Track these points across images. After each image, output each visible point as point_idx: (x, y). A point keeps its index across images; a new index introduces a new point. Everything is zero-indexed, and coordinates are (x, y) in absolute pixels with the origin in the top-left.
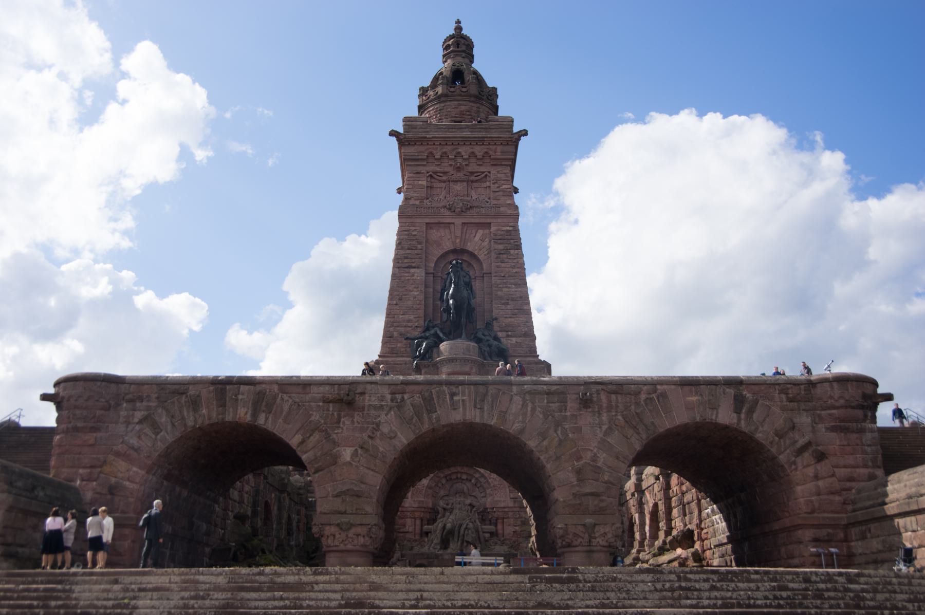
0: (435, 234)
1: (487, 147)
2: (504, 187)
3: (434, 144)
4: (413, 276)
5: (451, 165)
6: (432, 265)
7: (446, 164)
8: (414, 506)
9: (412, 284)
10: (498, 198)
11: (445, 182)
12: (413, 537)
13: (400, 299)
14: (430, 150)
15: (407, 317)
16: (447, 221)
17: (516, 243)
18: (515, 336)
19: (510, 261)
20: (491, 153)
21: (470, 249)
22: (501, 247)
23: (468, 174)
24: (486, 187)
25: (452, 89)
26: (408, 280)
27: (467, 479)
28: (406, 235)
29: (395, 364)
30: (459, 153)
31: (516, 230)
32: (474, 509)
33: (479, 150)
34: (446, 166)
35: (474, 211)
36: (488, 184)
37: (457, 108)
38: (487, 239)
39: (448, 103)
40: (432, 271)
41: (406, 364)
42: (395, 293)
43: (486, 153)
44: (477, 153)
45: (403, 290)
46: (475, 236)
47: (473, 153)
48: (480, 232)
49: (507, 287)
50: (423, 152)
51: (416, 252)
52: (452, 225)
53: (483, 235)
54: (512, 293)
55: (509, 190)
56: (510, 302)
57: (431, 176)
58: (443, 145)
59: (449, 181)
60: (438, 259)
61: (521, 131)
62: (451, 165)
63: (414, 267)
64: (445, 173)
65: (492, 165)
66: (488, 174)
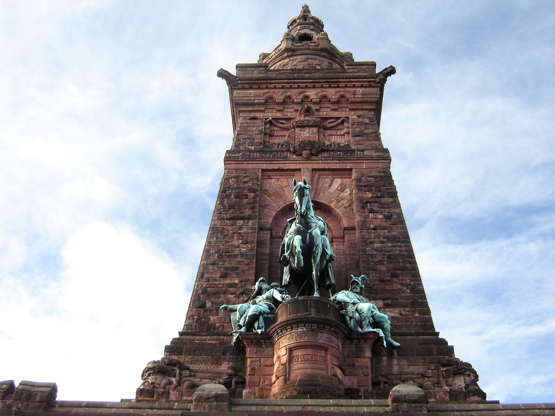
0: (273, 183)
1: (343, 90)
3: (275, 88)
4: (240, 228)
5: (296, 110)
6: (271, 220)
7: (292, 110)
9: (238, 239)
10: (361, 142)
14: (271, 94)
15: (228, 281)
16: (292, 166)
17: (390, 190)
20: (348, 96)
21: (323, 201)
22: (369, 195)
23: (319, 119)
24: (344, 135)
25: (299, 44)
26: (234, 233)
30: (307, 97)
31: (390, 176)
33: (332, 93)
34: (290, 112)
36: (345, 130)
37: (304, 61)
38: (348, 191)
39: (294, 58)
40: (269, 226)
43: (343, 96)
44: (330, 96)
46: (330, 186)
47: (325, 97)
48: (338, 182)
50: (259, 96)
52: (298, 172)
53: (341, 184)
57: (270, 122)
58: (286, 88)
59: (294, 128)
60: (277, 214)
61: (386, 69)
62: (296, 110)
63: (243, 218)
64: (289, 119)
65: (351, 110)
66: (346, 119)
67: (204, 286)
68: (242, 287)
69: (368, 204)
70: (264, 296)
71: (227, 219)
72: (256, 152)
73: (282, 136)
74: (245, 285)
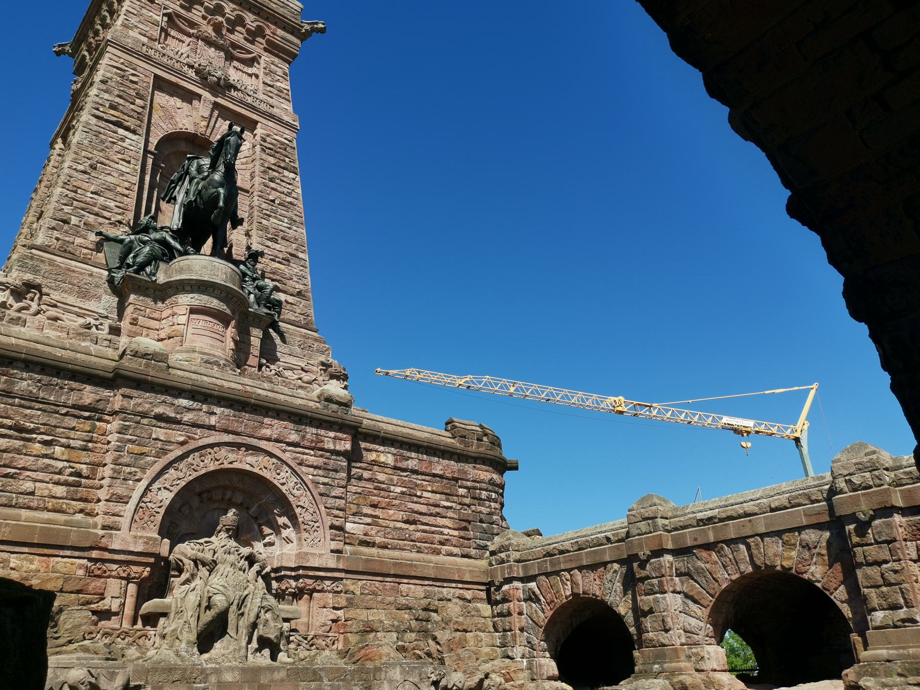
2: (278, 84)
4: (123, 140)
8: (132, 549)
11: (189, 35)
12: (118, 626)
13: (93, 167)
18: (285, 292)
19: (284, 184)
20: (268, 32)
27: (241, 504)
28: (116, 74)
29: (69, 270)
32: (256, 567)
35: (234, 93)
41: (91, 275)
42: (84, 154)
45: (101, 154)
49: (275, 218)
51: (132, 106)
54: (284, 229)
55: (285, 91)
56: (280, 241)
57: (168, 15)
63: (127, 129)
64: (192, 24)
65: (265, 50)
67: (70, 196)
68: (119, 214)
69: (270, 171)
70: (152, 236)
71: (107, 121)
72: (152, 49)
73: (180, 41)
74: (124, 213)
